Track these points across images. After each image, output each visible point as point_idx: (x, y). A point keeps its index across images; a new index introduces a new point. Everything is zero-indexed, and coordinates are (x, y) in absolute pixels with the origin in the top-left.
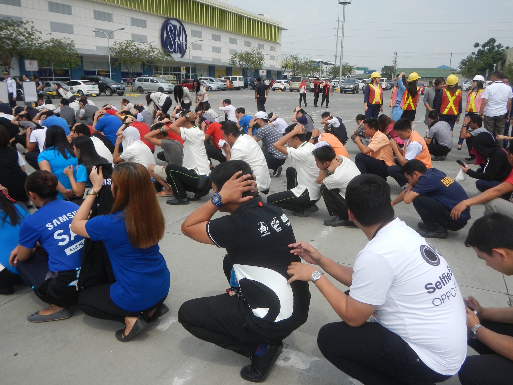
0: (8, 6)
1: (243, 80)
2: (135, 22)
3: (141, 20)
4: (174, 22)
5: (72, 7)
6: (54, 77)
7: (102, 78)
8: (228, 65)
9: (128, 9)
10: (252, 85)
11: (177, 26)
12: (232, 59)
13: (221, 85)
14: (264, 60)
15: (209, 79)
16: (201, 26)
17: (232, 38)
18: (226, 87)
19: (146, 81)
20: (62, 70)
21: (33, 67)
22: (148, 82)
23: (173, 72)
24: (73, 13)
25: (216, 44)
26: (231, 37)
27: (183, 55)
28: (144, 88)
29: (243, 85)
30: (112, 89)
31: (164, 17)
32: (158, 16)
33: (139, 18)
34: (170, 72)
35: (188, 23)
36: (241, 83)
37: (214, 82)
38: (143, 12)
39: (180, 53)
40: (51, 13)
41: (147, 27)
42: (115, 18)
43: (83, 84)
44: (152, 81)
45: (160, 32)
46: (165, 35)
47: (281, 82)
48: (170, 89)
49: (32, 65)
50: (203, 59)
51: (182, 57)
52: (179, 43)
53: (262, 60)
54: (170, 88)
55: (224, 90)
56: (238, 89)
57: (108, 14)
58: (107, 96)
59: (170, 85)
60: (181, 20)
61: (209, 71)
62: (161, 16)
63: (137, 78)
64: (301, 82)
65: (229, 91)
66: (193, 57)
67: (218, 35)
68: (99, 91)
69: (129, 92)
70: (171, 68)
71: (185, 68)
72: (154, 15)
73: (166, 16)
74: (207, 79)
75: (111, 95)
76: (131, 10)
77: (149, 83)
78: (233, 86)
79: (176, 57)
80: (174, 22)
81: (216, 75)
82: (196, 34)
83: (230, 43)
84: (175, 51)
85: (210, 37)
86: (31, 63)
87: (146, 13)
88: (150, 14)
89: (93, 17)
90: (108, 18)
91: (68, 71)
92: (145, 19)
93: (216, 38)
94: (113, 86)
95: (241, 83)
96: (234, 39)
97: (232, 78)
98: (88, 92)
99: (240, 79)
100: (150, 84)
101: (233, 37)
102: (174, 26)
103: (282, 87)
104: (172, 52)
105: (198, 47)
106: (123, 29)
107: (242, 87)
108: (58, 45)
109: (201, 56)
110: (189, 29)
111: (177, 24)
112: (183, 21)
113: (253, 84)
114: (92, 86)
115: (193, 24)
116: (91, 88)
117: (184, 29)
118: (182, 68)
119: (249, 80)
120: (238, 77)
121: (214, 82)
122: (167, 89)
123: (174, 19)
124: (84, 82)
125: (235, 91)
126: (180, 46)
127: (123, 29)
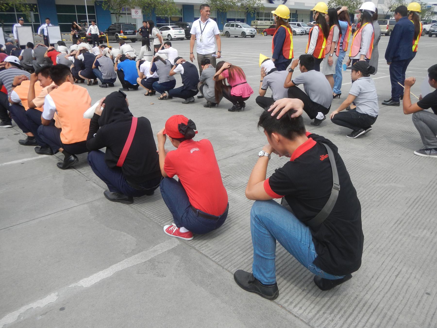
6: (169, 24)
7: (189, 24)
12: (329, 3)
13: (307, 29)
14: (361, 4)
15: (297, 24)
19: (233, 26)
21: (138, 15)
22: (234, 27)
28: (230, 33)
34: (271, 18)
37: (301, 26)
43: (171, 29)
44: (237, 26)
48: (251, 33)
49: (137, 14)
50: (306, 5)
53: (360, 3)
54: (252, 32)
59: (252, 29)
63: (226, 24)
64: (386, 25)
66: (295, 3)
68: (185, 35)
69: (221, 36)
74: (295, 24)
77: (235, 28)
86: (136, 12)
91: (182, 18)
98: (175, 36)
100: (235, 29)
109: (304, 2)
114: (179, 31)
116: (178, 32)
121: (301, 26)
122: (249, 33)
124: (172, 27)
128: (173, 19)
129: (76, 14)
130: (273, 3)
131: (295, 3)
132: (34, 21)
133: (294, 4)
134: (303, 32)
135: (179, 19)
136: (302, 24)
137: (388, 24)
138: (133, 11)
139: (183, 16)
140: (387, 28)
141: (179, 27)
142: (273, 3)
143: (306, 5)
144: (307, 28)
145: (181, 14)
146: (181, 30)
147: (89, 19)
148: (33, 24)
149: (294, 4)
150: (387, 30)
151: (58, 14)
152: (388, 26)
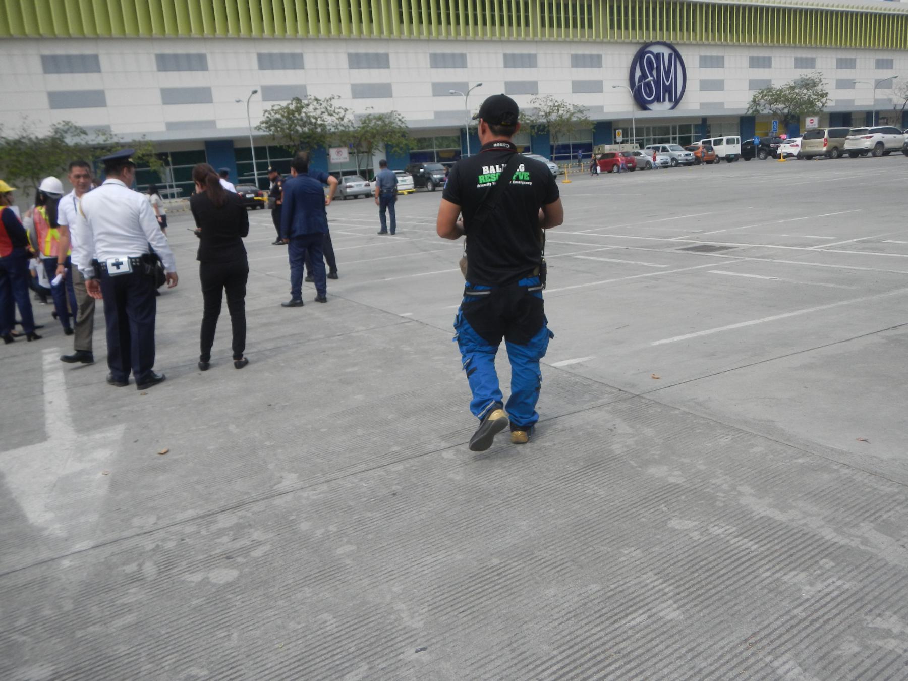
0: (372, 70)
1: (738, 143)
2: (578, 61)
3: (591, 56)
4: (656, 50)
8: (743, 113)
9: (565, 42)
10: (765, 150)
11: (663, 54)
13: (680, 156)
16: (722, 45)
17: (801, 58)
18: (689, 158)
20: (451, 151)
23: (652, 137)
24: (469, 65)
25: (761, 74)
26: (799, 56)
27: (677, 102)
29: (739, 152)
30: (434, 180)
31: (638, 43)
32: (623, 43)
35: (691, 45)
36: (736, 149)
37: (668, 151)
38: (595, 43)
39: (670, 100)
40: (434, 70)
41: (604, 65)
42: (541, 60)
45: (629, 69)
46: (638, 73)
47: (794, 141)
50: (726, 107)
51: (673, 108)
52: (668, 84)
55: (688, 164)
56: (729, 159)
57: (529, 56)
58: (429, 191)
60: (674, 42)
61: (741, 128)
62: (631, 43)
65: (704, 167)
66: (702, 105)
67: (764, 58)
70: (648, 128)
71: (621, 131)
72: (616, 43)
73: (641, 41)
75: (433, 190)
76: (572, 42)
78: (712, 155)
79: (660, 110)
80: (656, 50)
81: (756, 132)
82: (705, 62)
83: (796, 67)
84: (658, 99)
85: (745, 62)
87: (602, 43)
88: (609, 43)
89: (501, 64)
90: (530, 61)
92: (600, 53)
93: (755, 63)
94: (435, 176)
95: (736, 149)
96: (806, 59)
97: (715, 141)
99: (729, 142)
101: (804, 56)
102: (657, 56)
103: (795, 151)
104: (651, 102)
105: (706, 85)
106: (480, 85)
107: (736, 155)
110: (690, 57)
111: (666, 52)
112: (678, 44)
113: (767, 149)
115: (703, 45)
117: (678, 56)
118: (617, 131)
119: (757, 141)
120: (725, 138)
123: (658, 43)
125: (725, 165)
126: (668, 90)
127: (480, 85)
128: (442, 155)
129: (269, 160)
130: (649, 110)
131: (702, 105)
132: (169, 179)
133: (697, 107)
134: (666, 163)
135: (453, 154)
136: (671, 147)
137: (826, 135)
138: (333, 152)
139: (463, 148)
140: (825, 145)
141: (404, 173)
142: (649, 110)
143: (726, 107)
144: (679, 153)
145: (459, 145)
146: (405, 178)
147: (258, 170)
148: (167, 184)
149: (697, 107)
150: (825, 149)
151: (238, 165)
152: (826, 140)
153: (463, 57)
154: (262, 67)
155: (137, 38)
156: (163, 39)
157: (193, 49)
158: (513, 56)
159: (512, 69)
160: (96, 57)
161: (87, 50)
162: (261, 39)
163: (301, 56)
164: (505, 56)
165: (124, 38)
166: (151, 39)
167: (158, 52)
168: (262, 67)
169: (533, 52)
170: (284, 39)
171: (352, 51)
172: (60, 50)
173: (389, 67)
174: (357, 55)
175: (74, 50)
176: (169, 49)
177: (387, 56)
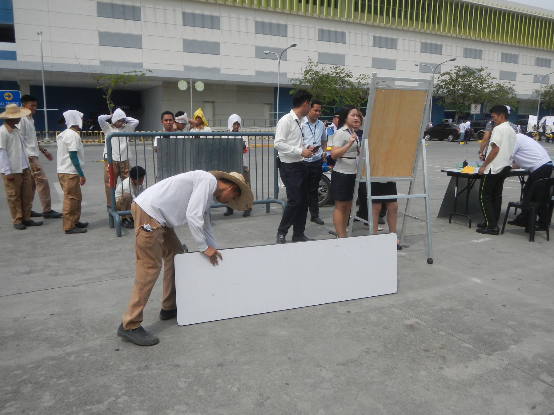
3: (546, 59)
5: (483, 52)
24: (483, 58)
33: (544, 57)
57: (515, 55)
76: (539, 50)
90: (513, 59)
108: (501, 90)
138: (473, 106)
147: (432, 114)
153: (481, 51)
154: (374, 46)
155: (312, 18)
156: (326, 20)
157: (339, 28)
158: (507, 54)
159: (504, 63)
160: (286, 26)
161: (282, 21)
162: (378, 27)
163: (396, 40)
164: (503, 54)
165: (305, 16)
166: (319, 19)
167: (320, 28)
168: (374, 46)
169: (517, 54)
170: (390, 29)
171: (424, 41)
172: (267, 19)
173: (441, 54)
174: (426, 43)
175: (275, 20)
176: (326, 27)
177: (441, 46)
